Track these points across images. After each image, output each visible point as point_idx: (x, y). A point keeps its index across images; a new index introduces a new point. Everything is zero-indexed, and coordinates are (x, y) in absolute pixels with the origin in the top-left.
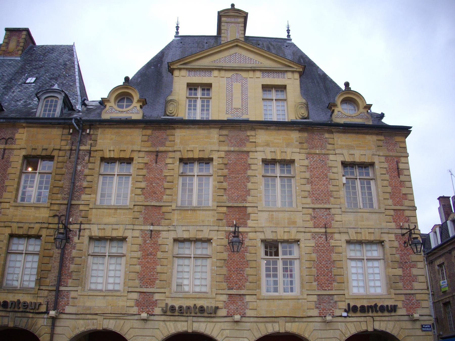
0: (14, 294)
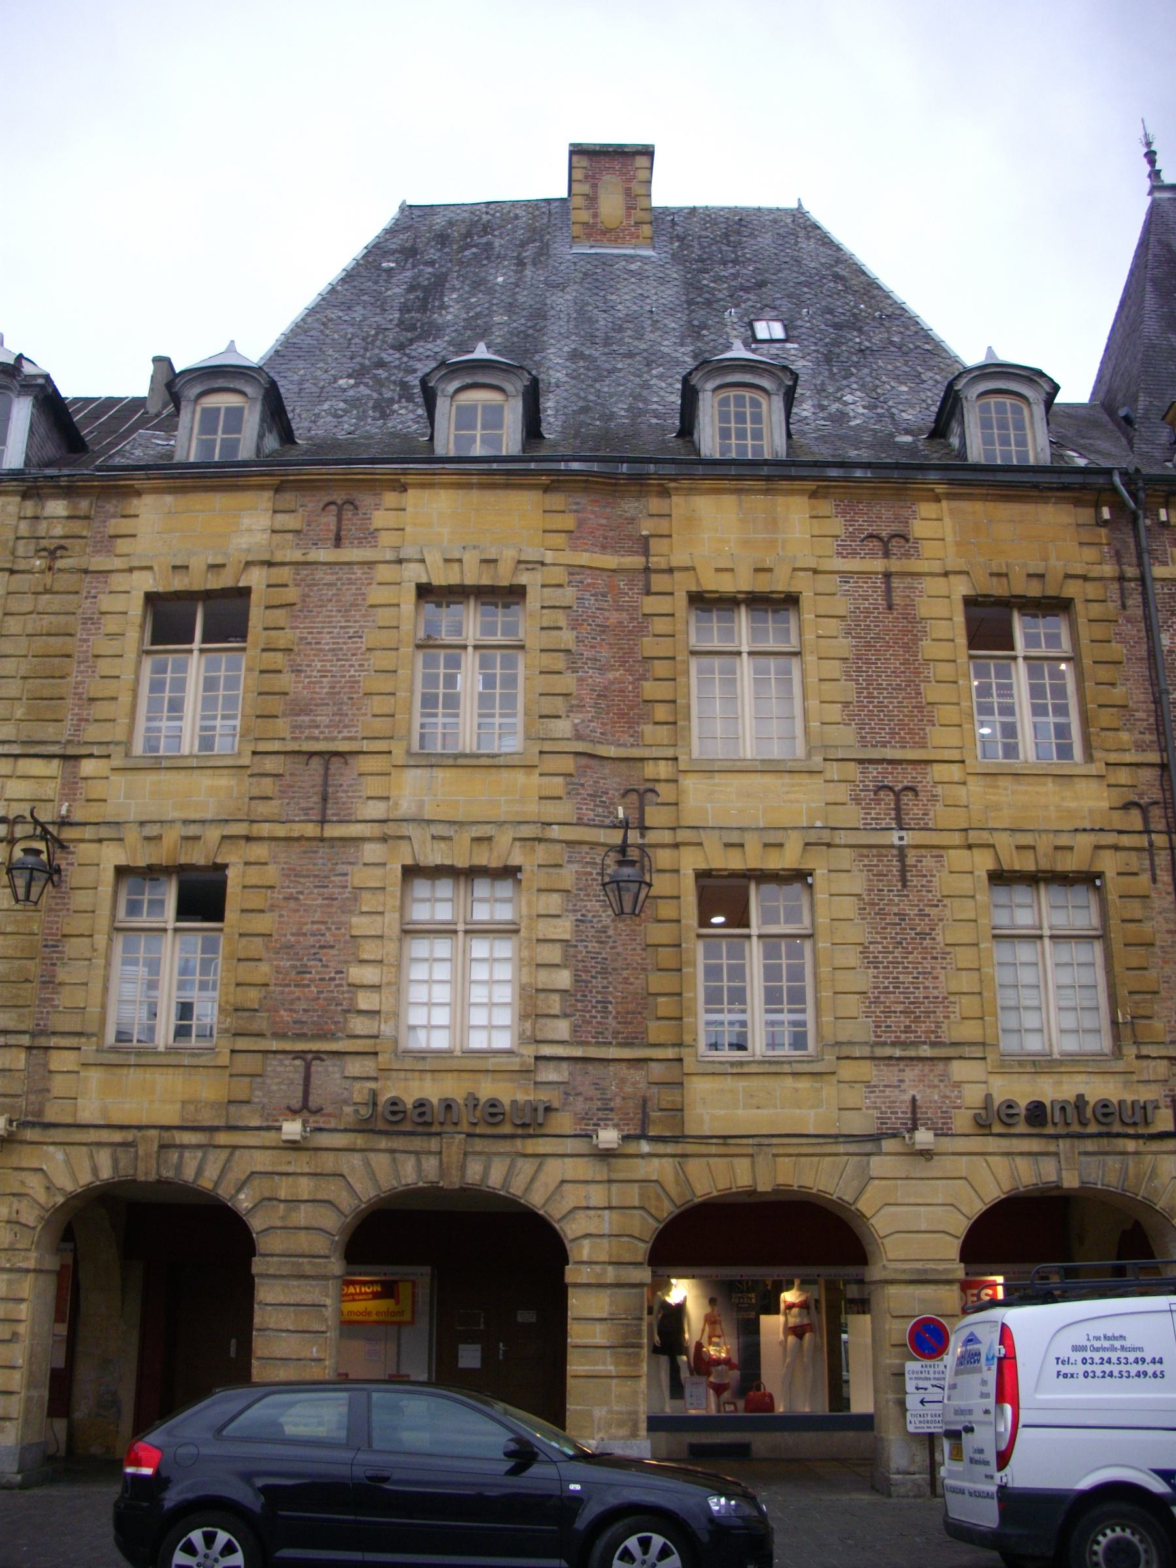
0: (1056, 1077)
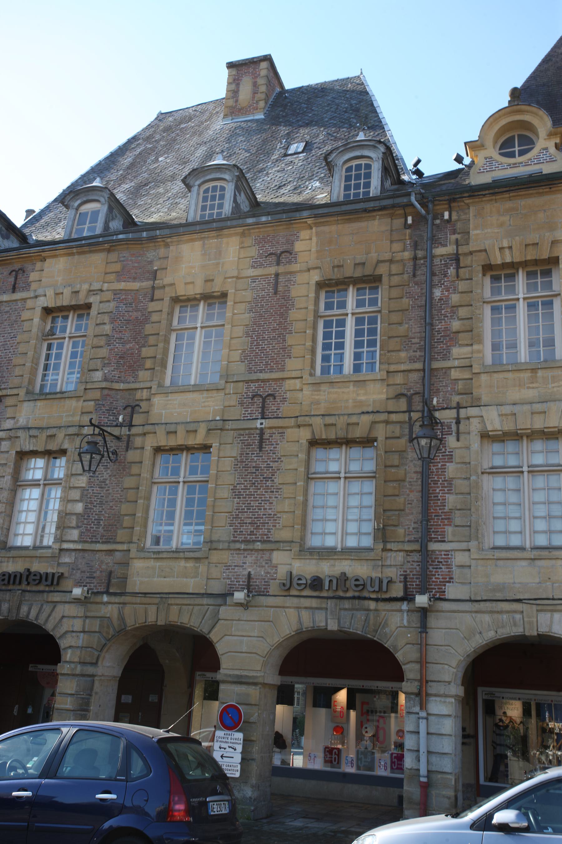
0: (332, 561)
